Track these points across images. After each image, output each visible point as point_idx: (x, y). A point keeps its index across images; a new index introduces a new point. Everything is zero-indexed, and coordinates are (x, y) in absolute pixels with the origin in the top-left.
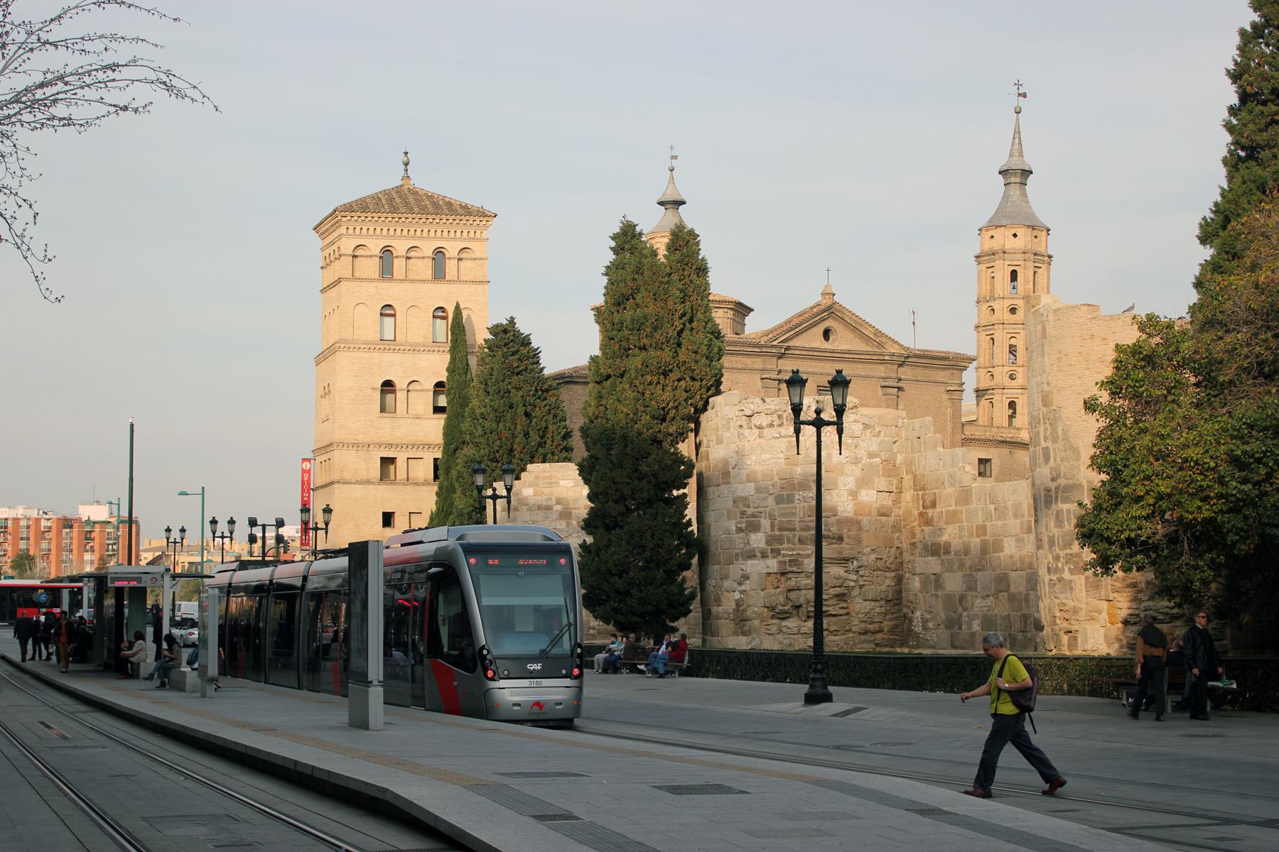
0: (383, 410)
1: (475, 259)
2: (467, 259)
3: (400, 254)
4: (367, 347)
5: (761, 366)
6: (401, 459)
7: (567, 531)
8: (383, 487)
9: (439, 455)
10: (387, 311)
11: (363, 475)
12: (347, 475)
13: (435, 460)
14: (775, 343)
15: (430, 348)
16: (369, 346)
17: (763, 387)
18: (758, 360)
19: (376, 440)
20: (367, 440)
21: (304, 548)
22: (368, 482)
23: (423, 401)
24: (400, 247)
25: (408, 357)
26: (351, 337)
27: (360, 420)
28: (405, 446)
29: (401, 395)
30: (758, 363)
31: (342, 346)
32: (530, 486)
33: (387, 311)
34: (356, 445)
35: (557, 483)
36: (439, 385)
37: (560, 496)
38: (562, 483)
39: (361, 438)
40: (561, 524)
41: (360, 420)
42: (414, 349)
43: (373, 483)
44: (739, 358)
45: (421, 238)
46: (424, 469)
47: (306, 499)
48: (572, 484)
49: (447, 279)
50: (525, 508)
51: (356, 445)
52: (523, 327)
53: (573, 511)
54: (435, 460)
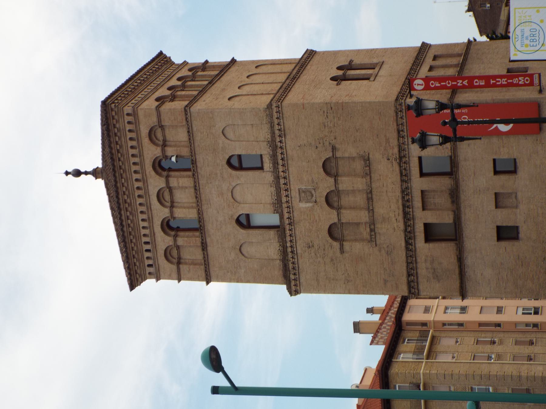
47: (465, 83)
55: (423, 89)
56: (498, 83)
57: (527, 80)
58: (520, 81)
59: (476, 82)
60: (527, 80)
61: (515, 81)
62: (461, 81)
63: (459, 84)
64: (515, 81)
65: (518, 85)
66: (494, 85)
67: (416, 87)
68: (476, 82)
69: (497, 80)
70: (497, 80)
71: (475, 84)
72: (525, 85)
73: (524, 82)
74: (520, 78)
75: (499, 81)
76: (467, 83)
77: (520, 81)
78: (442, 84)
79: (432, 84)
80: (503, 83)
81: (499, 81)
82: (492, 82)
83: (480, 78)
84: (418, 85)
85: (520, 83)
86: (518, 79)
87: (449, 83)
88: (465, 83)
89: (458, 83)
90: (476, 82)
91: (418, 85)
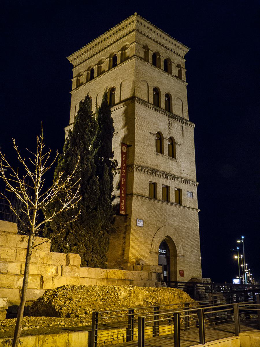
57: (123, 207)
58: (123, 203)
60: (123, 207)
62: (124, 172)
68: (123, 180)
69: (124, 191)
70: (124, 191)
73: (122, 206)
74: (124, 204)
75: (123, 192)
76: (124, 175)
77: (123, 203)
80: (122, 194)
81: (123, 192)
84: (124, 148)
86: (124, 203)
88: (124, 174)
89: (124, 170)
91: (124, 148)
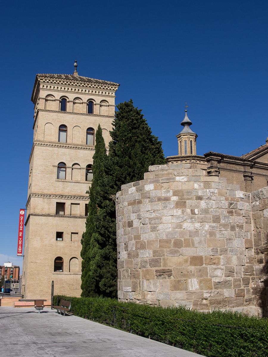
0: (58, 178)
1: (109, 106)
2: (104, 106)
3: (70, 100)
4: (51, 144)
5: (243, 170)
6: (68, 203)
7: (182, 218)
8: (57, 218)
9: (87, 202)
10: (63, 128)
11: (46, 212)
12: (38, 211)
13: (86, 205)
14: (250, 159)
15: (84, 147)
16: (52, 145)
17: (245, 180)
18: (242, 167)
19: (54, 193)
20: (49, 193)
21: (19, 254)
22: (49, 215)
23: (80, 174)
24: (71, 97)
25: (72, 151)
26: (42, 139)
27: (46, 182)
28: (70, 197)
29: (69, 170)
30: (242, 168)
31: (38, 143)
32: (150, 183)
33: (63, 128)
34: (43, 195)
35: (174, 178)
36: (89, 166)
37: (176, 189)
38: (178, 178)
39: (46, 192)
40: (177, 212)
41: (46, 182)
42: (76, 147)
43: (52, 216)
44: (234, 166)
45: (81, 93)
46: (80, 210)
47: (21, 229)
48: (186, 179)
49: (94, 114)
50: (148, 200)
51: (43, 195)
52: (136, 106)
53: (187, 201)
54: (86, 205)
55: (20, 214)
56: (20, 241)
57: (20, 251)
59: (21, 233)
61: (20, 247)
62: (22, 228)
63: (21, 227)
64: (20, 247)
65: (18, 248)
66: (19, 239)
67: (21, 211)
71: (20, 233)
72: (18, 250)
78: (22, 221)
79: (22, 217)
82: (20, 239)
83: (22, 234)
85: (19, 249)
87: (21, 223)
90: (21, 233)
